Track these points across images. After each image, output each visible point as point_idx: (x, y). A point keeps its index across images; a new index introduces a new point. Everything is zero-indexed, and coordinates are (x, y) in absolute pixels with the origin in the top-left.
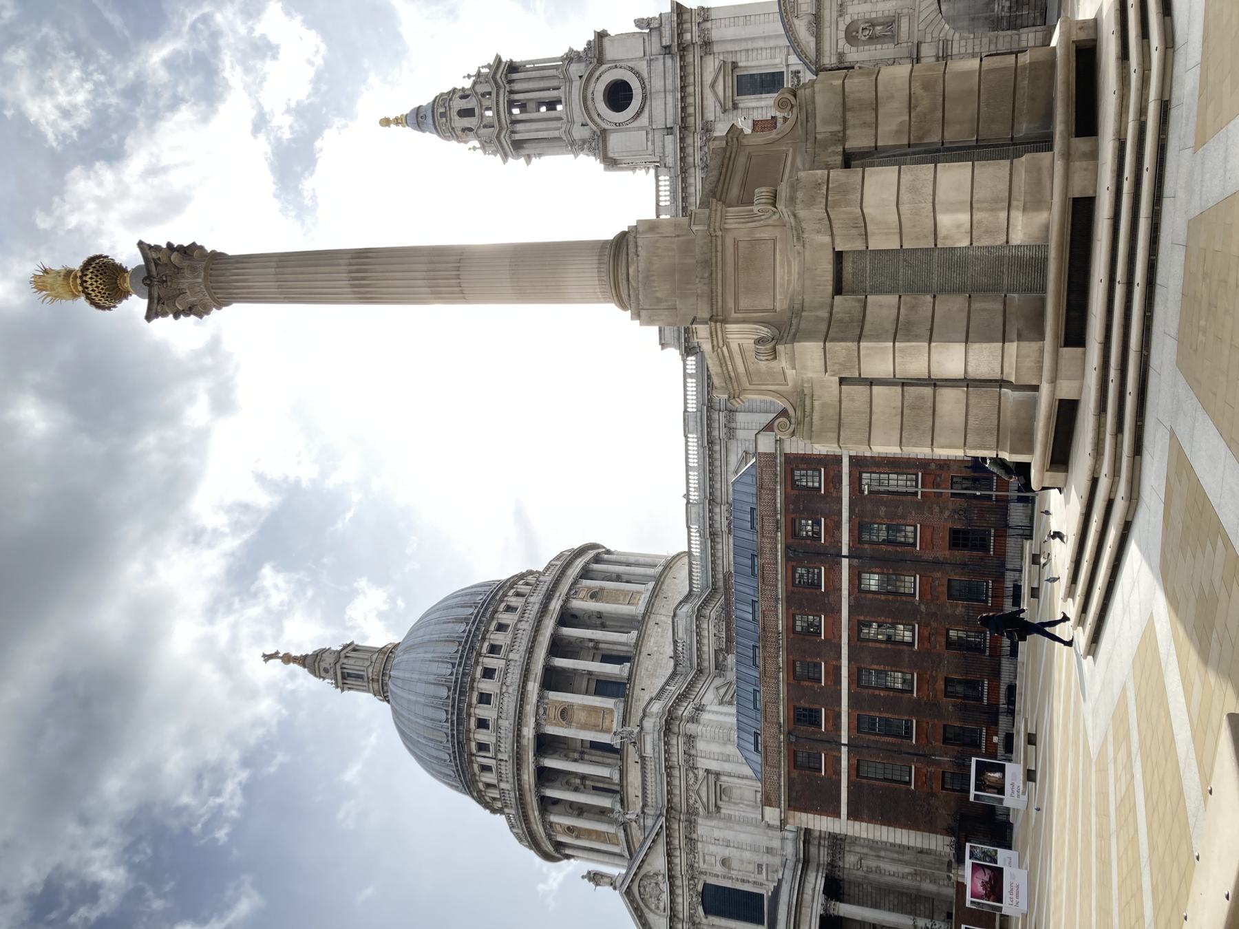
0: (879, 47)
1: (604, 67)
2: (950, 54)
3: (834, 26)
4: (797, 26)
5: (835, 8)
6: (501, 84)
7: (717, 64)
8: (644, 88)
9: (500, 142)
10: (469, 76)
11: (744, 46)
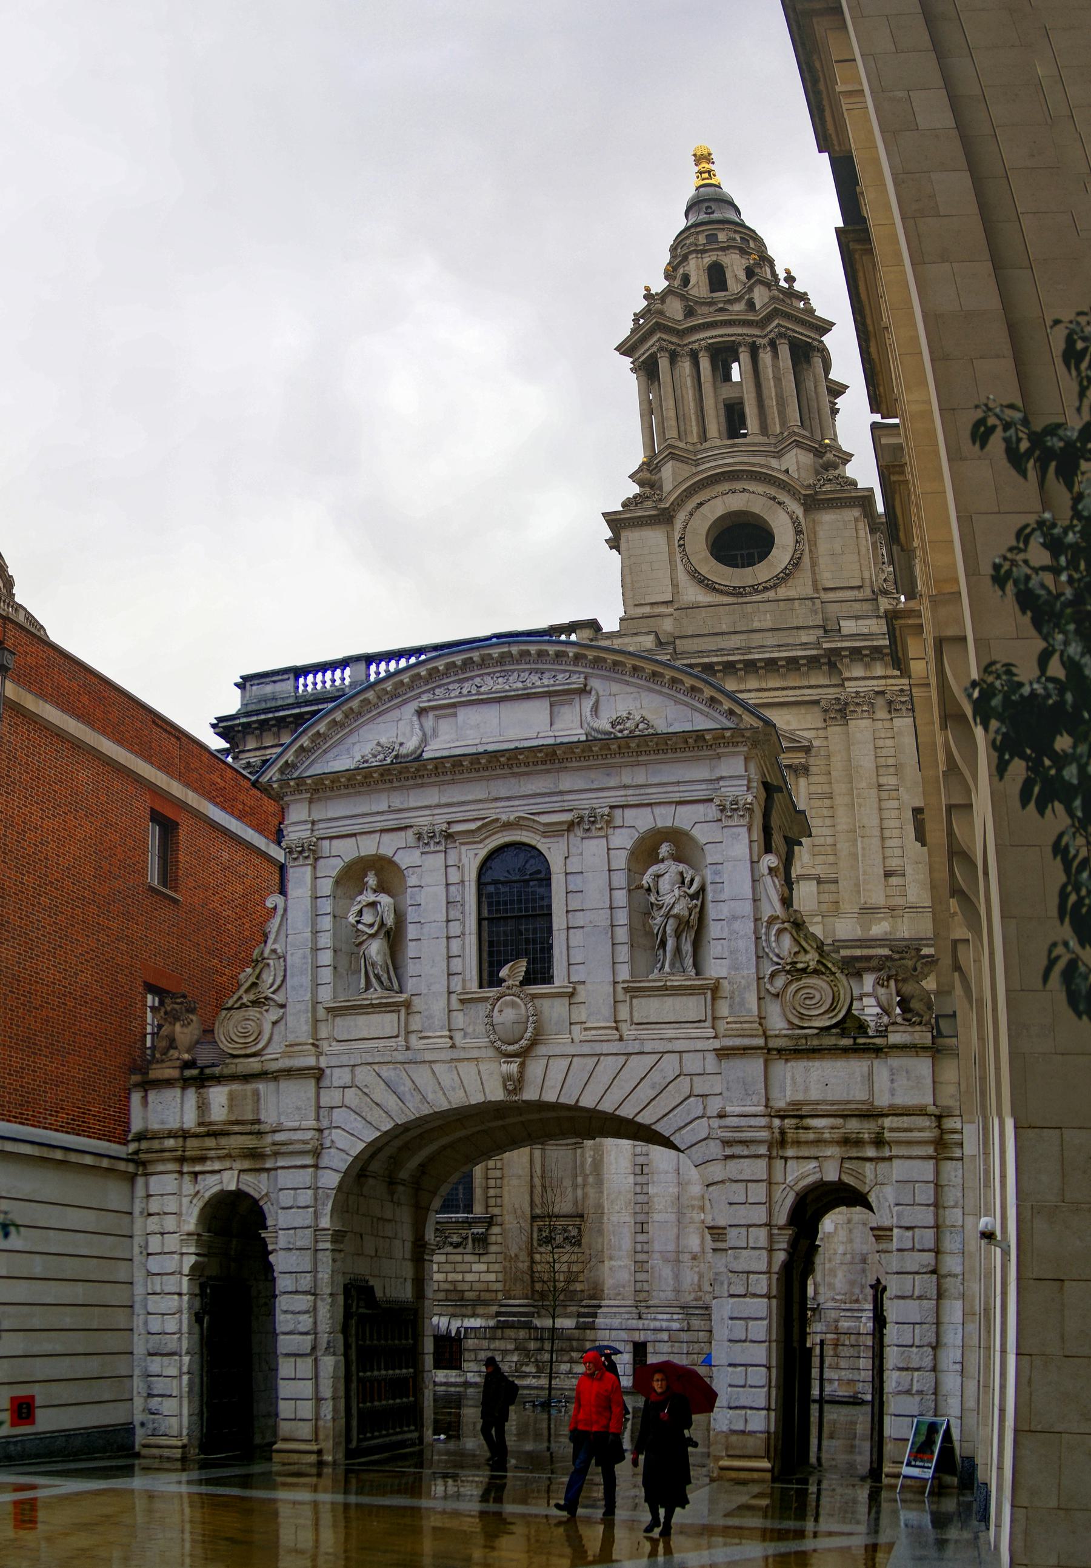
0: (326, 958)
1: (799, 512)
3: (391, 821)
4: (396, 714)
5: (440, 820)
6: (769, 329)
7: (805, 734)
8: (755, 589)
9: (651, 333)
10: (790, 279)
11: (839, 788)
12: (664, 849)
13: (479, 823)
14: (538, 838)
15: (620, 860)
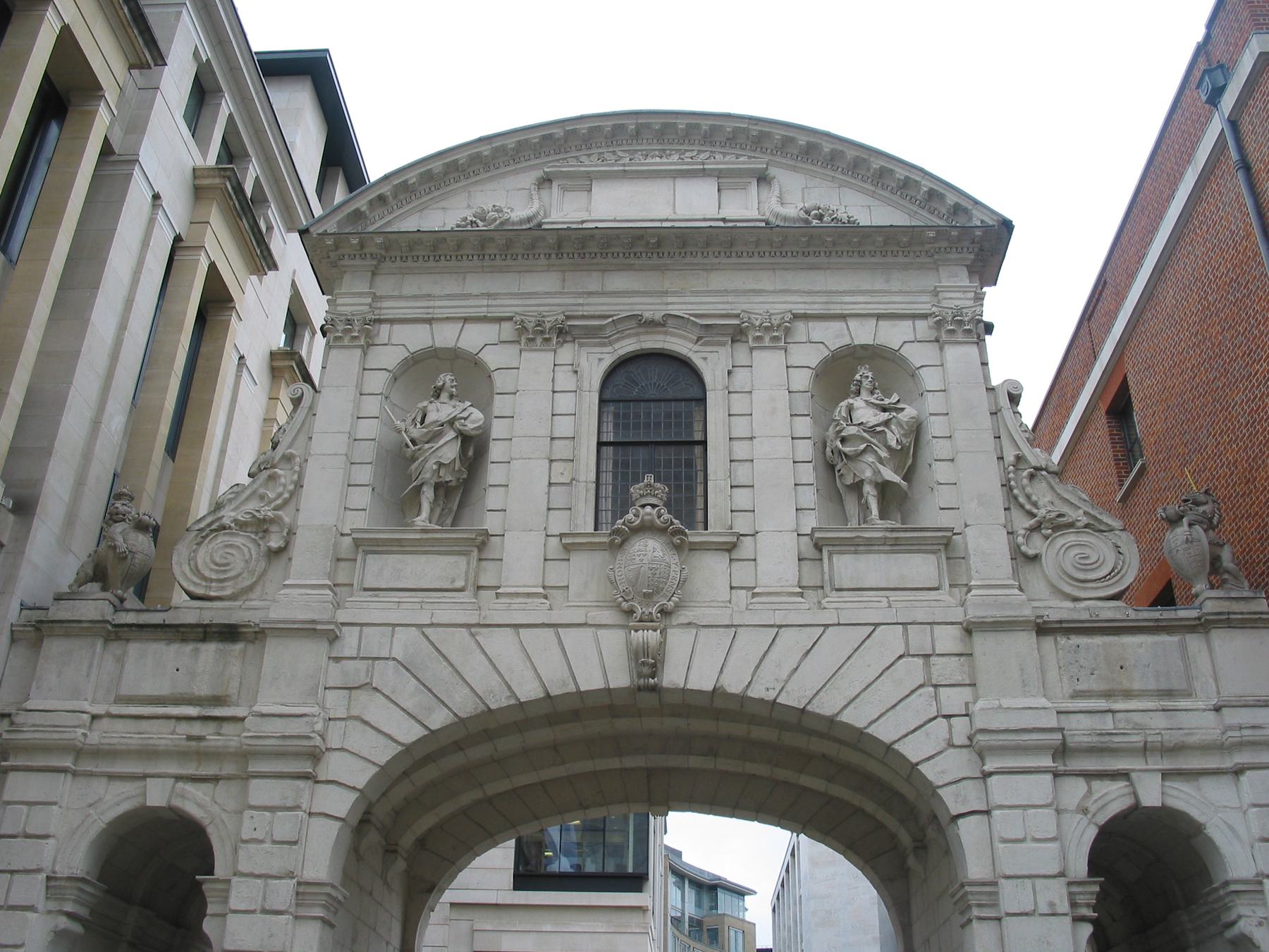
0: (364, 474)
2: (254, 767)
12: (864, 373)
13: (610, 320)
14: (690, 345)
15: (802, 380)
